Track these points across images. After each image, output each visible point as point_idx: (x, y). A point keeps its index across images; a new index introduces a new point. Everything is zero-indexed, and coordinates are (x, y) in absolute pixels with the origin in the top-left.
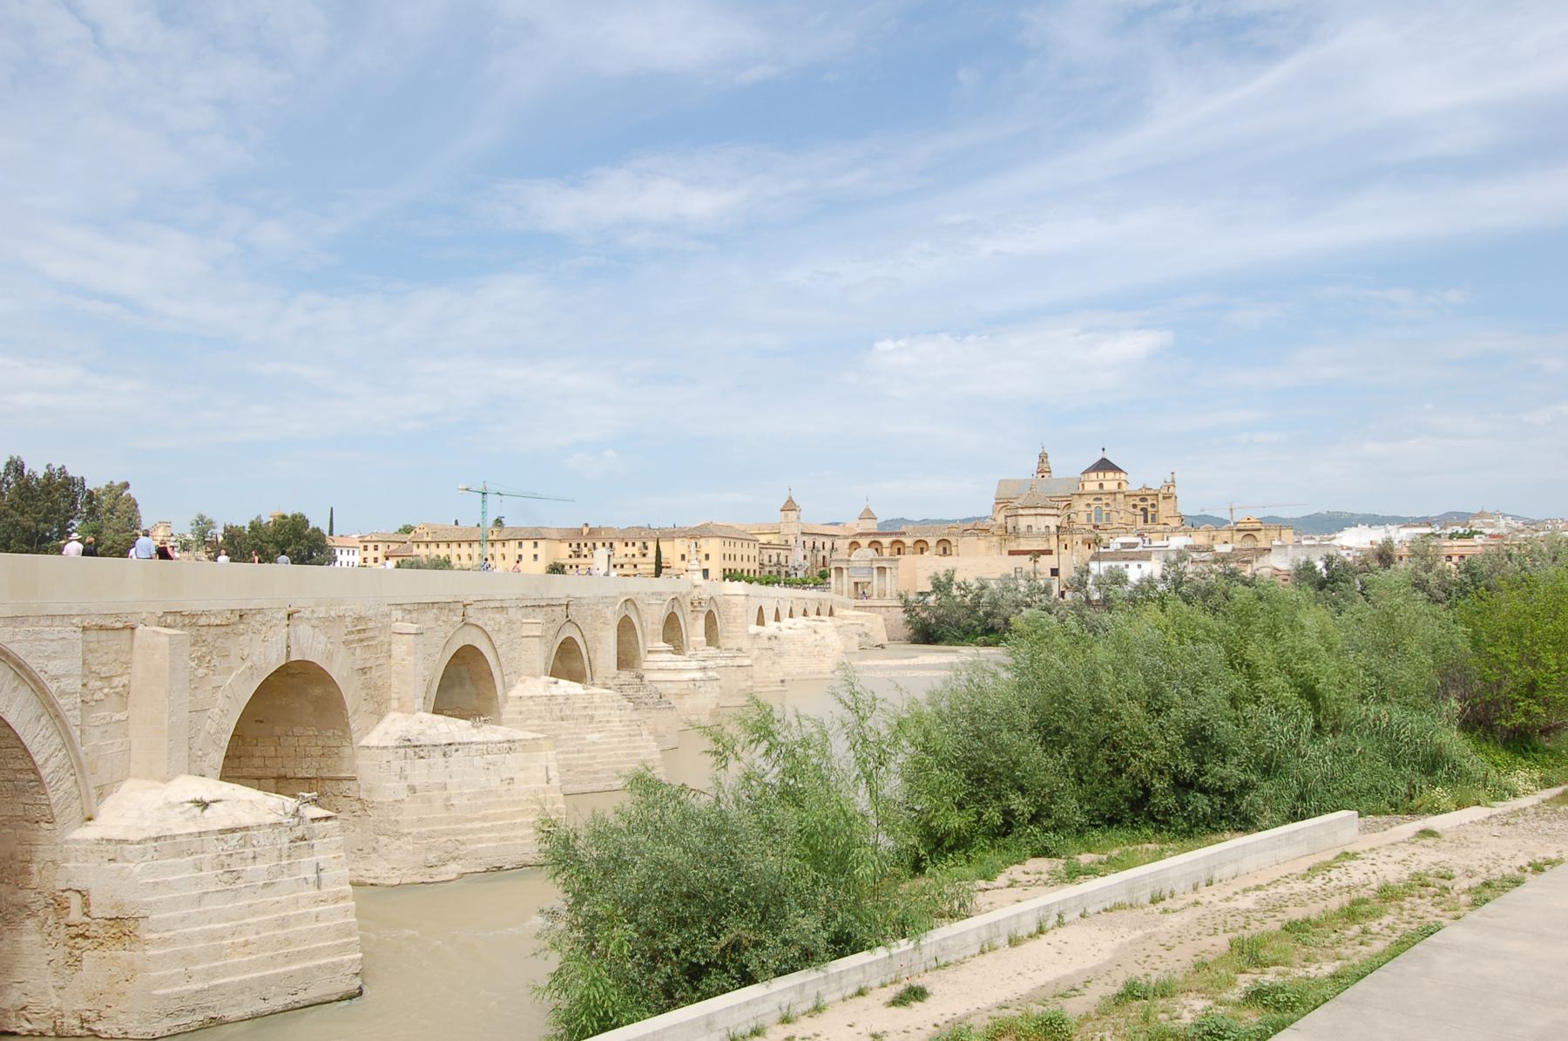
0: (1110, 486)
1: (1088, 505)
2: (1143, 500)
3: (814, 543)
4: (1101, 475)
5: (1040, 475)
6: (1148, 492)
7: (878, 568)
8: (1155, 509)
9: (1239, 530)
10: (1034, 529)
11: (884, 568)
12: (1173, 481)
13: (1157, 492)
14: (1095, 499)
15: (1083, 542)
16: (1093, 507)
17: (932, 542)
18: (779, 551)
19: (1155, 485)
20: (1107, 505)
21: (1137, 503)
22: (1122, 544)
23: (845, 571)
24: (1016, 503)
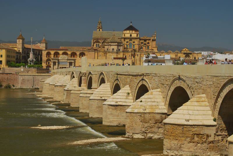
1: (127, 42)
3: (28, 51)
4: (131, 31)
5: (98, 29)
6: (147, 38)
8: (149, 44)
9: (184, 54)
11: (72, 63)
13: (150, 38)
14: (129, 40)
17: (78, 53)
18: (17, 54)
20: (134, 42)
21: (143, 42)
22: (153, 57)
24: (109, 40)
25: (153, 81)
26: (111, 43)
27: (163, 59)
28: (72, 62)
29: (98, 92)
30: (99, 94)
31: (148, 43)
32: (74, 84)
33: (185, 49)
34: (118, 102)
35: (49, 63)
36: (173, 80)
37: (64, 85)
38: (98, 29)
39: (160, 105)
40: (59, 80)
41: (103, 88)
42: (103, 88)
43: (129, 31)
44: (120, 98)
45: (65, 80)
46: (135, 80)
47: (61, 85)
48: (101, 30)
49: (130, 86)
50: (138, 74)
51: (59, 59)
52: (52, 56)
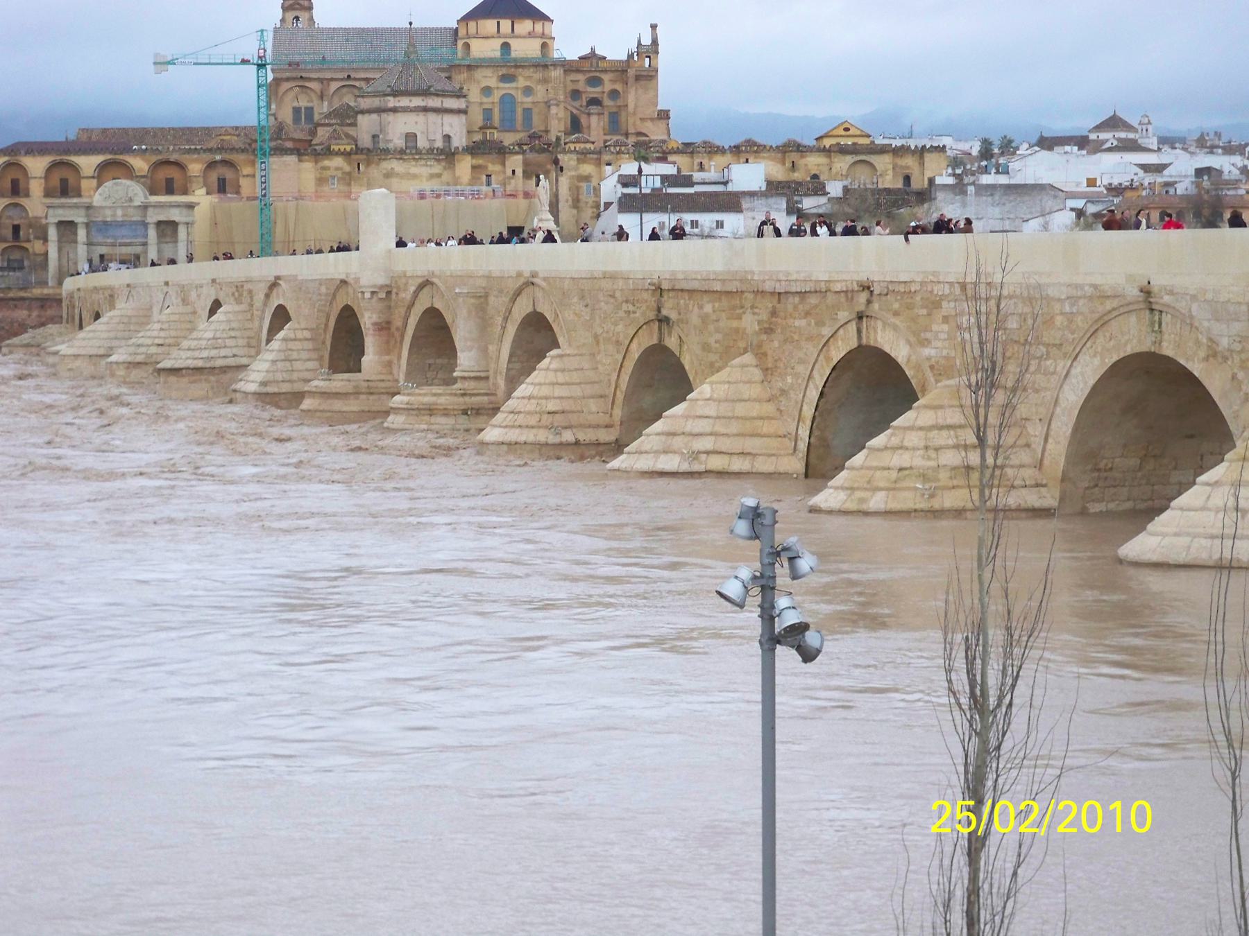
0: (525, 48)
1: (487, 91)
2: (595, 81)
4: (506, 24)
5: (290, 15)
7: (159, 223)
8: (619, 102)
10: (422, 143)
11: (173, 225)
12: (655, 42)
15: (524, 172)
16: (496, 96)
19: (616, 50)
20: (528, 91)
21: (581, 86)
23: (82, 234)
25: (945, 327)
26: (395, 93)
27: (720, 188)
28: (176, 219)
29: (530, 398)
30: (541, 413)
31: (614, 94)
32: (295, 355)
33: (846, 125)
34: (703, 457)
35: (16, 229)
36: (1100, 318)
37: (219, 363)
38: (290, 15)
39: (1012, 467)
40: (162, 334)
41: (561, 378)
42: (561, 378)
43: (494, 22)
44: (708, 429)
45: (218, 335)
46: (797, 323)
47: (200, 364)
48: (304, 16)
49: (761, 355)
50: (823, 287)
51: (95, 204)
52: (36, 187)
